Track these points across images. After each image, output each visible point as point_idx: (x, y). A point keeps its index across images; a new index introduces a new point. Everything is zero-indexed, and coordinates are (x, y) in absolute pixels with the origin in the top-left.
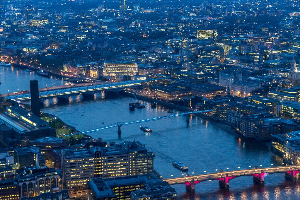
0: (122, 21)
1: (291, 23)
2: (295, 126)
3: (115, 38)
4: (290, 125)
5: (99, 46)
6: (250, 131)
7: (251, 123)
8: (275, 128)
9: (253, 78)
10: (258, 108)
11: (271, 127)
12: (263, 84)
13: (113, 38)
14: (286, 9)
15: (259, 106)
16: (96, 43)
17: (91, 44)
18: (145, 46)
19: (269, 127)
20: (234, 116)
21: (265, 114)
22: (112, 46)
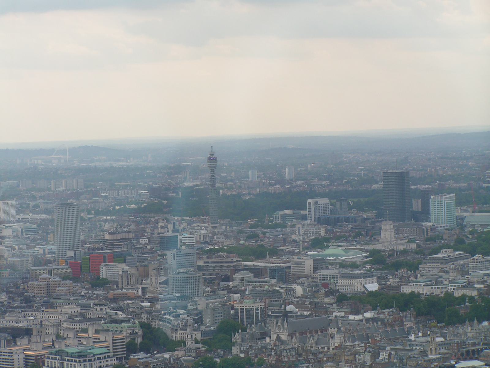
0: (392, 253)
3: (368, 315)
5: (311, 343)
13: (359, 317)
16: (301, 334)
17: (284, 337)
18: (474, 344)
22: (356, 343)
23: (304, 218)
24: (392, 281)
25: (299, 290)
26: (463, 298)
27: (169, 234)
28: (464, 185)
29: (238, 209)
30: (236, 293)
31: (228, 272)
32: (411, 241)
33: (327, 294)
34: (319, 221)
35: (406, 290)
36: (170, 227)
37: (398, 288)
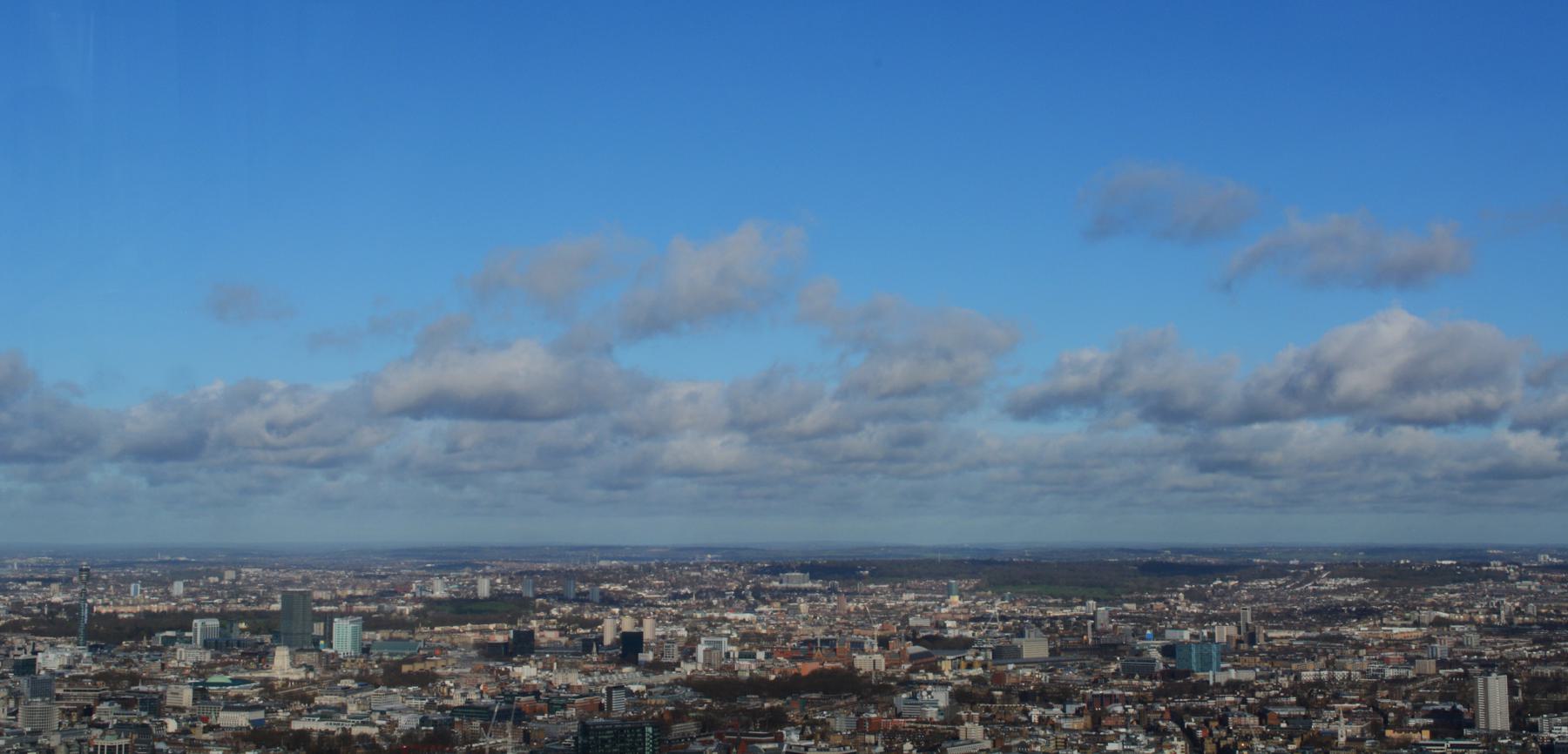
1: (942, 698)
14: (931, 641)
23: (189, 641)
24: (282, 715)
25: (172, 726)
26: (363, 737)
27: (29, 656)
28: (373, 607)
29: (106, 634)
30: (98, 727)
31: (91, 702)
32: (310, 669)
33: (206, 730)
34: (207, 645)
35: (297, 725)
36: (30, 649)
37: (288, 723)
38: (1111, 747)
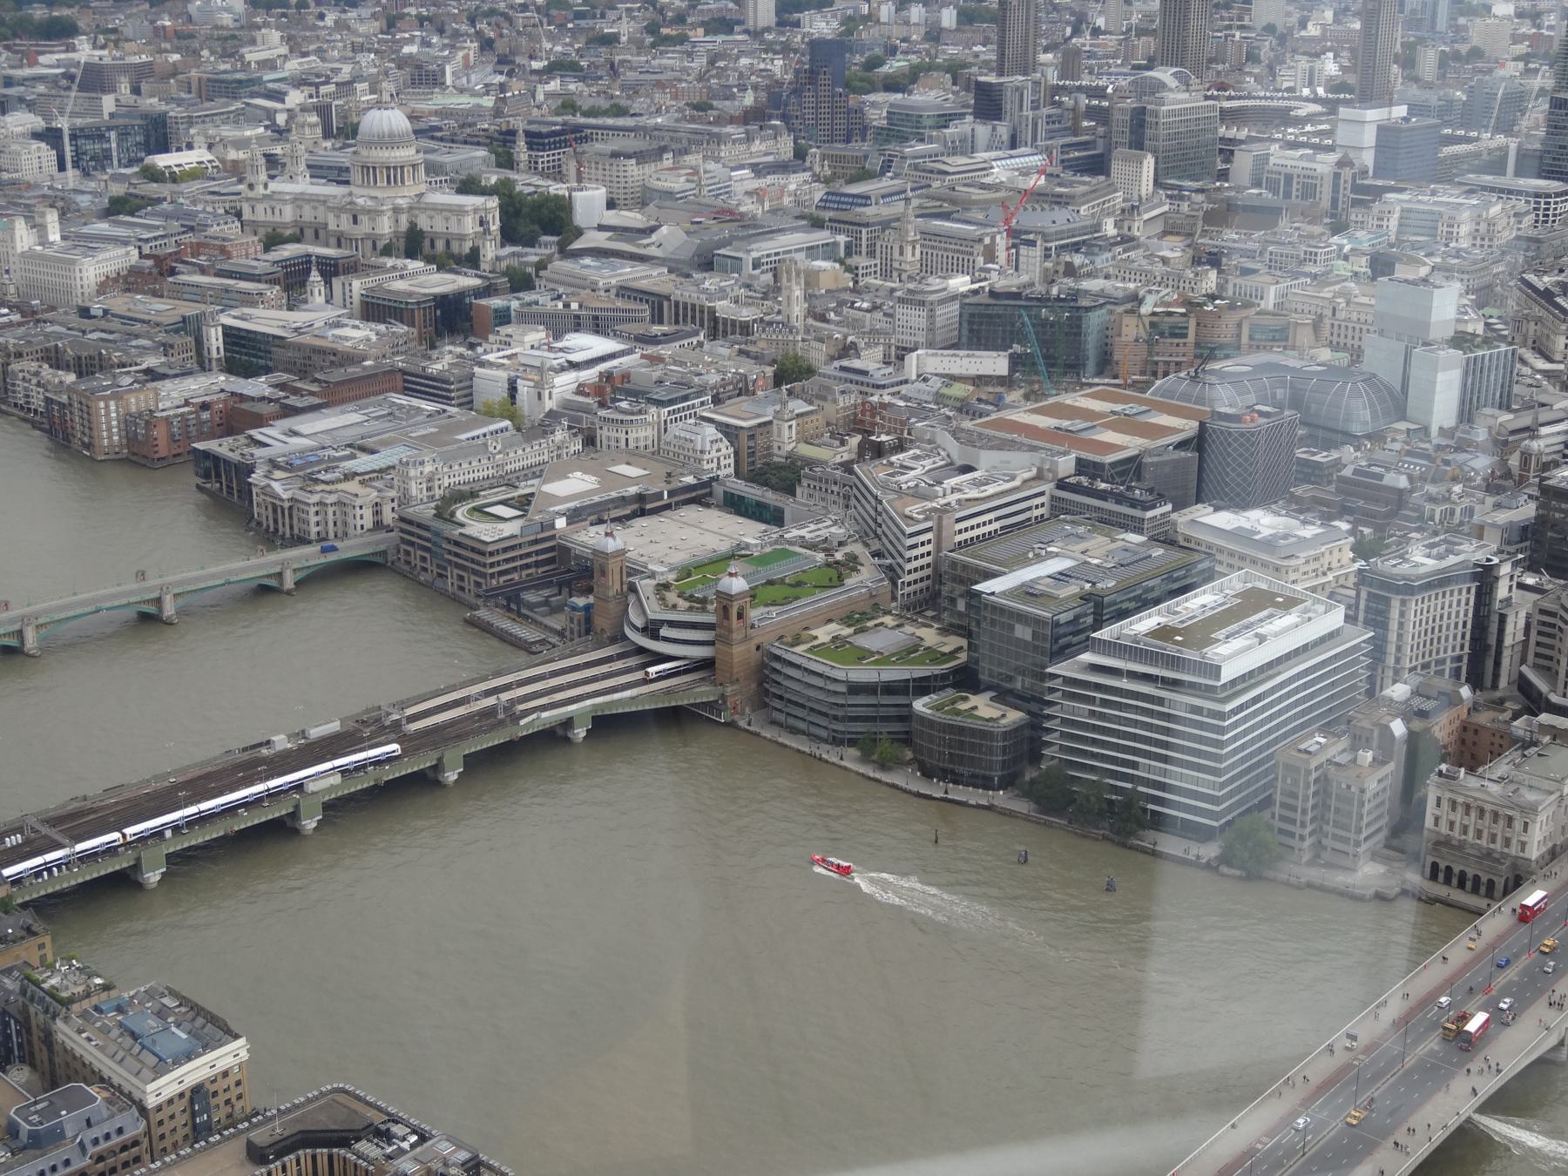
2: (277, 401)
4: (263, 399)
6: (110, 438)
7: (107, 407)
8: (205, 415)
9: (103, 227)
10: (134, 343)
11: (190, 413)
12: (146, 250)
15: (137, 337)
19: (182, 415)
20: (39, 384)
21: (162, 364)
38: (406, 50)
